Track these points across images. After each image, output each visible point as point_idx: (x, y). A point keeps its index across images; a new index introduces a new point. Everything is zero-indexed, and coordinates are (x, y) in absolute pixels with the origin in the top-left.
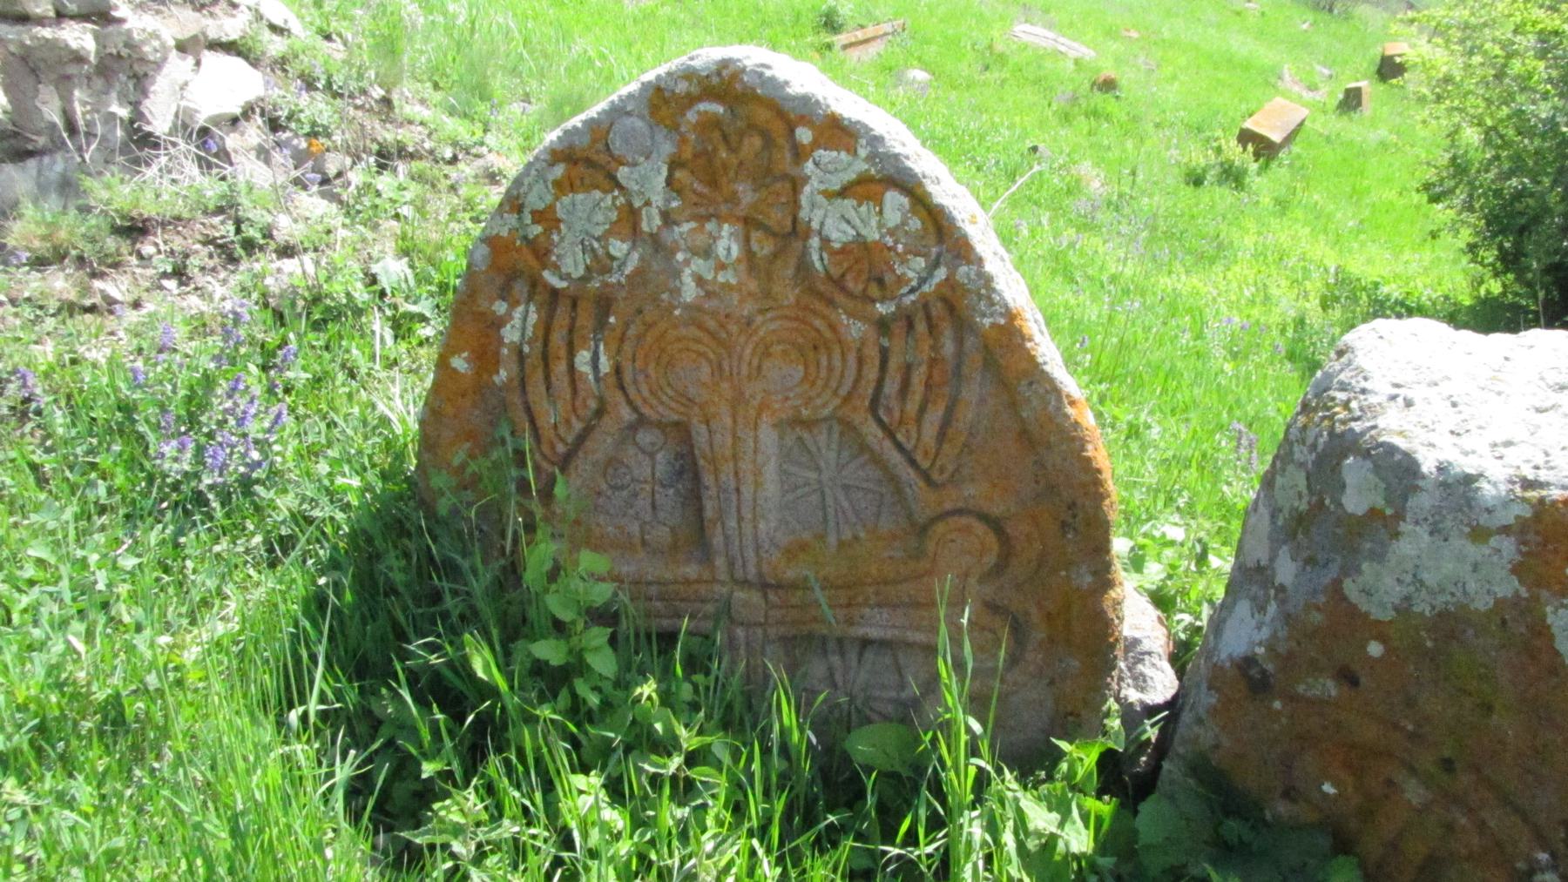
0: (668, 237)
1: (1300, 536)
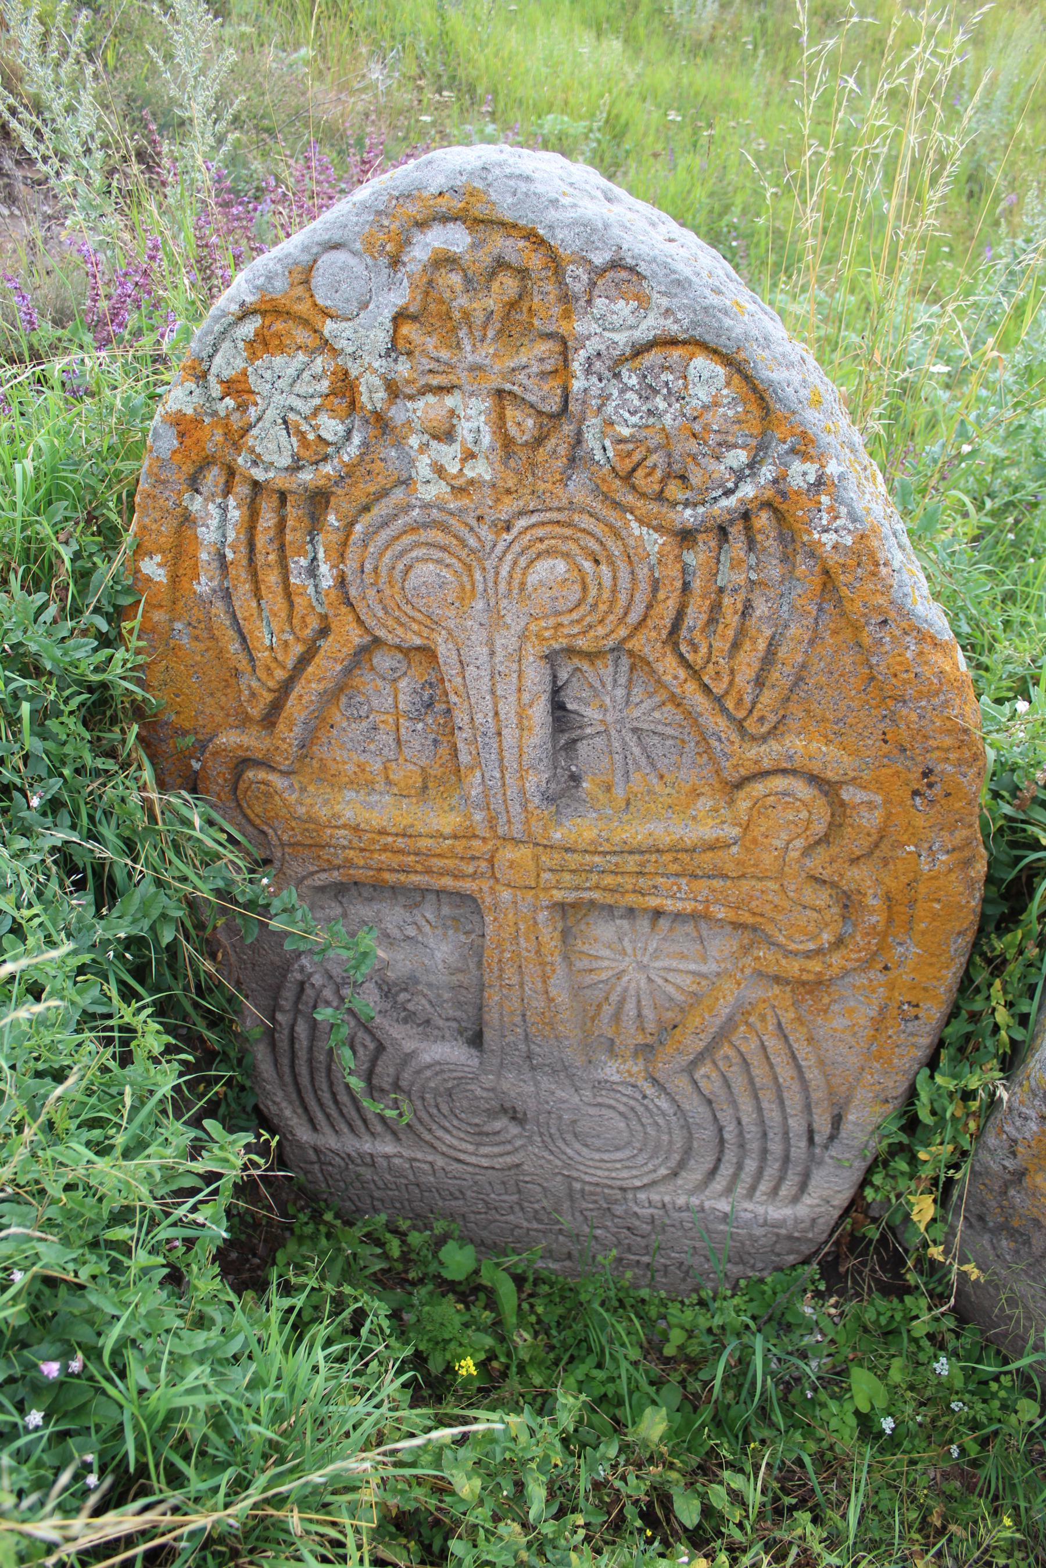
0: (398, 413)
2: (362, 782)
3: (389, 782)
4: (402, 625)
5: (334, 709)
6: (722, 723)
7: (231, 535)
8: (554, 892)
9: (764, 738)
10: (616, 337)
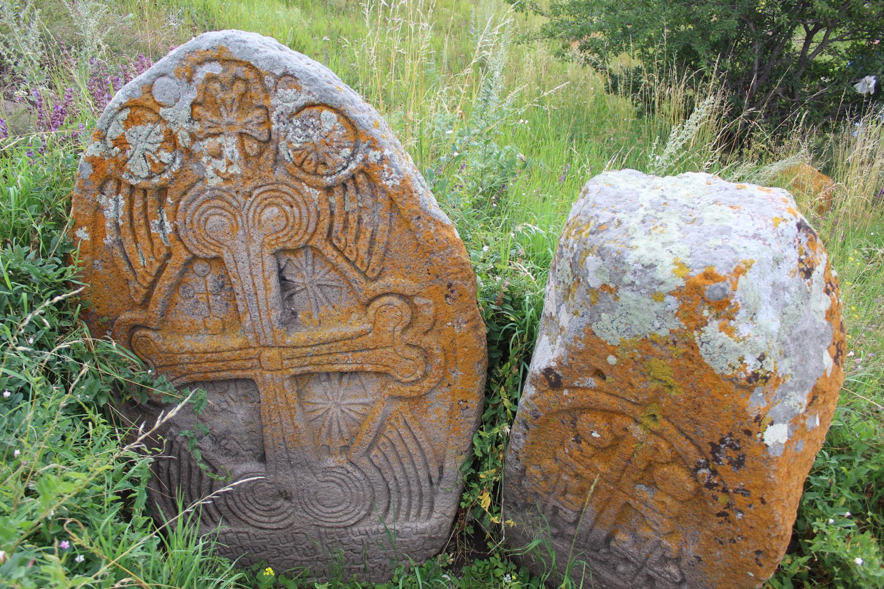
0: (196, 148)
1: (570, 299)
2: (194, 330)
3: (206, 328)
4: (206, 247)
5: (177, 295)
6: (356, 274)
7: (121, 213)
8: (291, 370)
9: (375, 280)
10: (288, 105)
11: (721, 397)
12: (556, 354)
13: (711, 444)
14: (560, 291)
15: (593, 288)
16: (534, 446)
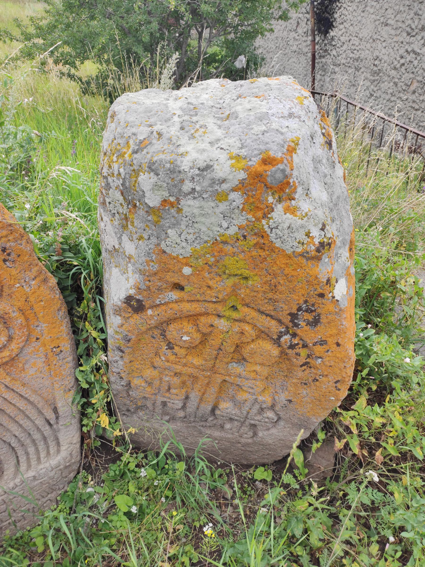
1: (130, 226)
11: (294, 273)
12: (132, 282)
13: (290, 314)
14: (116, 223)
15: (153, 208)
16: (132, 363)
